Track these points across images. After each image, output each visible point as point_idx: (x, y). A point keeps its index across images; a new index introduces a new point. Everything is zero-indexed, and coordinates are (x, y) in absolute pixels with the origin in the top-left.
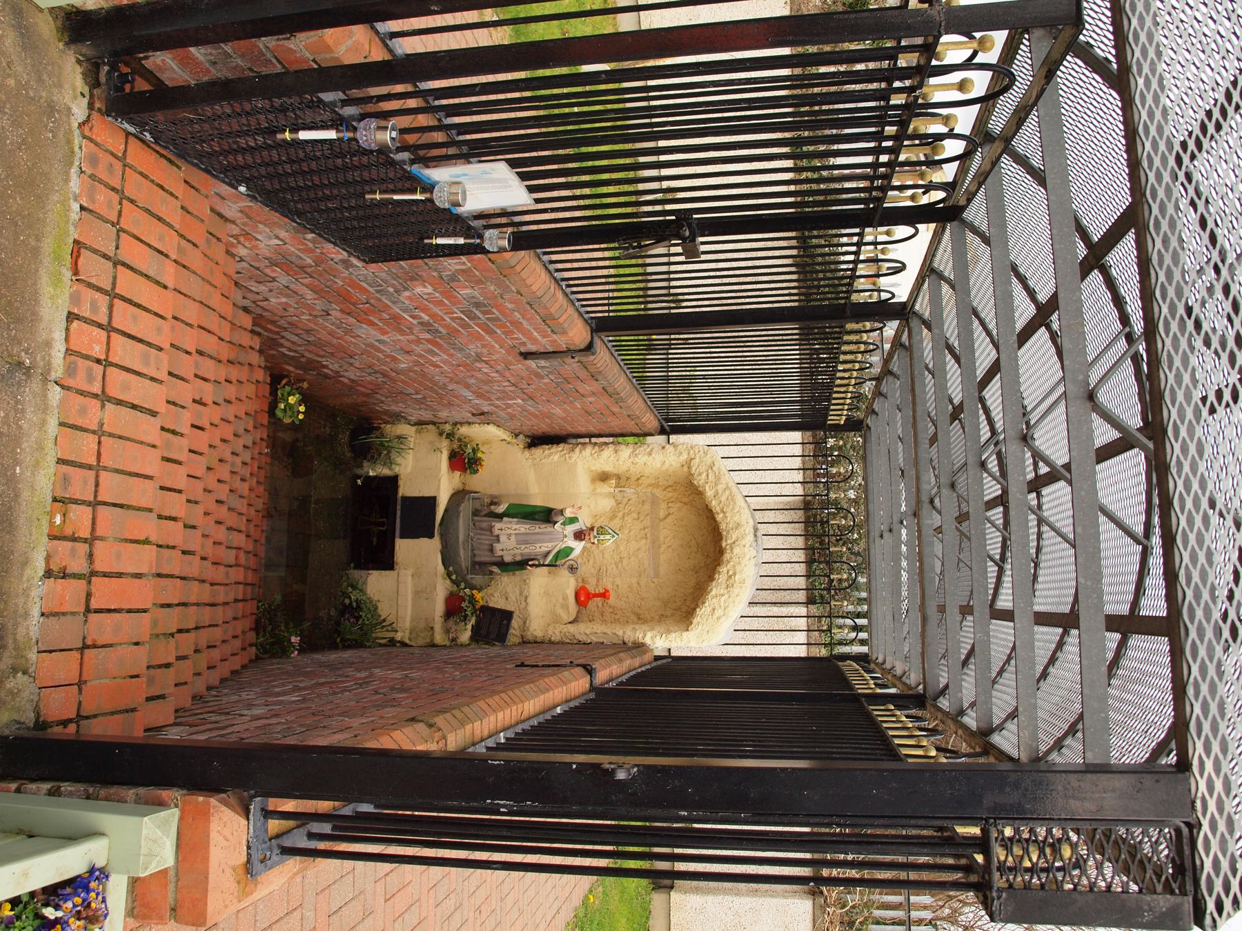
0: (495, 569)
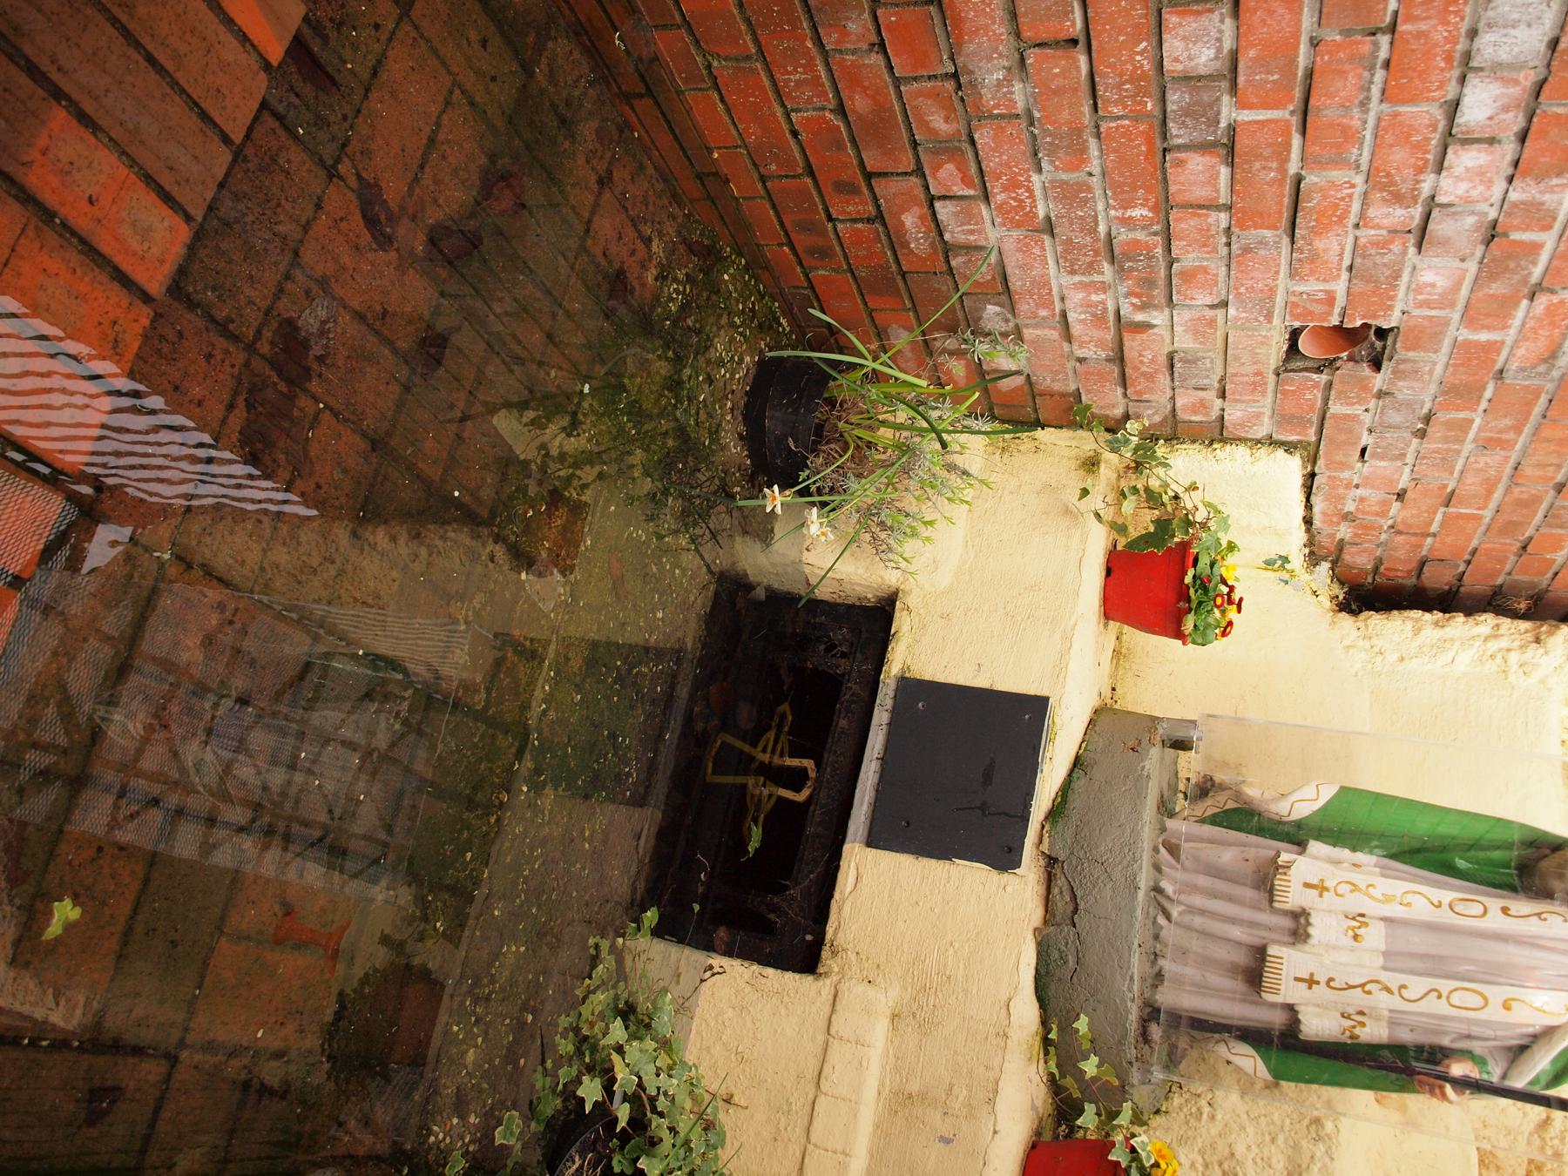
0: (1247, 1059)
